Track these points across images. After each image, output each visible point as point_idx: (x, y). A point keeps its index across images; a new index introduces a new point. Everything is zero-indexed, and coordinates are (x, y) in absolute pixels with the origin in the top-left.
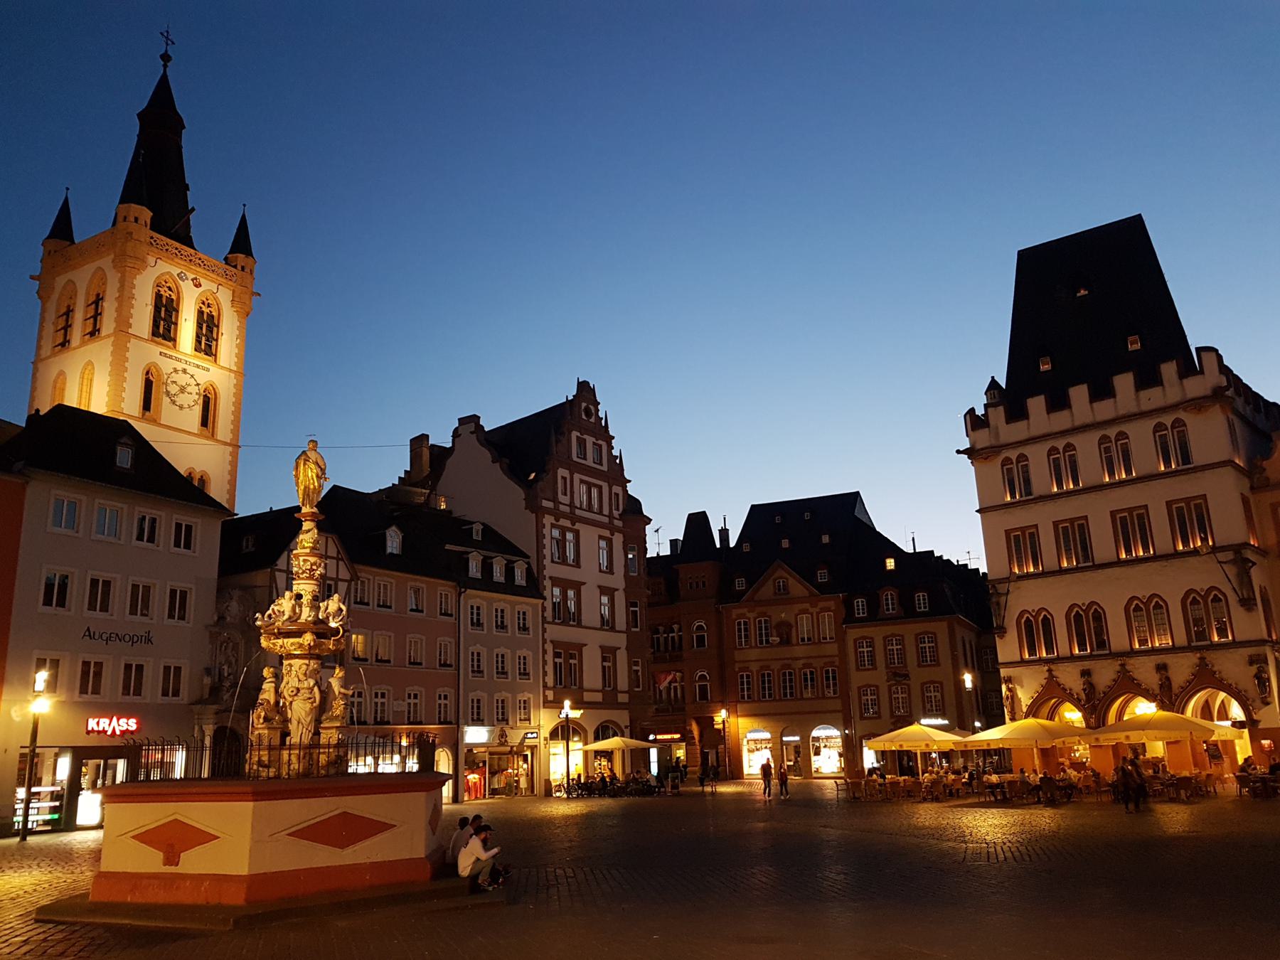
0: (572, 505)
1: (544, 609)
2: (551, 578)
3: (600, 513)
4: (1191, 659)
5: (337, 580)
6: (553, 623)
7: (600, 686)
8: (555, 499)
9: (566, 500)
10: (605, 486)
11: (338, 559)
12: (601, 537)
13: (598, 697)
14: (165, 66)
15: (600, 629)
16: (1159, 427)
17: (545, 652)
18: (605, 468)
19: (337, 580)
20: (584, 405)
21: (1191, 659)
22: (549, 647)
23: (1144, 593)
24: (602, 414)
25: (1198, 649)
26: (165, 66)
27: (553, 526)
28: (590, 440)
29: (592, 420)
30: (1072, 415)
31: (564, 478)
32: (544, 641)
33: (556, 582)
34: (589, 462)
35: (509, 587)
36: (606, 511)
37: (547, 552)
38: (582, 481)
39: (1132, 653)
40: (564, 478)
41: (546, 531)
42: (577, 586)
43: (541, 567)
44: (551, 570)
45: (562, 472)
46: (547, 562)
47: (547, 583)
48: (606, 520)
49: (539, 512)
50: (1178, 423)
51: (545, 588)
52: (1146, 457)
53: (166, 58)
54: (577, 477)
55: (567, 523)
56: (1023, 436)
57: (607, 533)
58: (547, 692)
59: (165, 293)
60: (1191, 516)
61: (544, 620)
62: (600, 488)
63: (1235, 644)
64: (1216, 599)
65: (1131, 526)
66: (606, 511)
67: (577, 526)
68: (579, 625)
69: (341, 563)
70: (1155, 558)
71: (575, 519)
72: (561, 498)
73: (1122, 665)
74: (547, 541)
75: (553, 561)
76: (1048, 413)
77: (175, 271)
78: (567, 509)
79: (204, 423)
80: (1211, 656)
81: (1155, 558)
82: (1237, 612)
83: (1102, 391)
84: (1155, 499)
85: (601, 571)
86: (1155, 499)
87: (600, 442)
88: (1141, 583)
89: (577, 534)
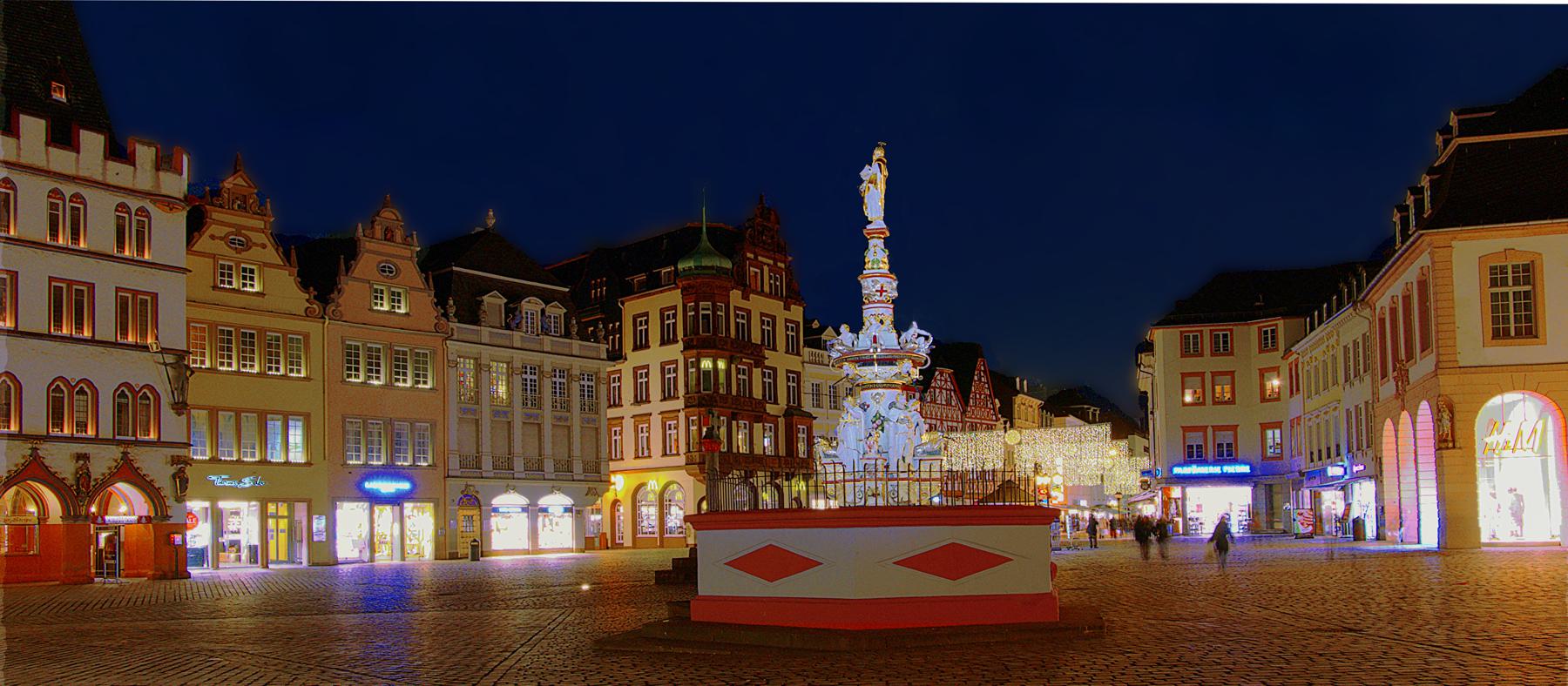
4: (115, 452)
16: (55, 193)
21: (115, 452)
23: (73, 376)
25: (120, 443)
30: (19, 148)
39: (47, 438)
50: (142, 211)
52: (100, 231)
56: (71, 171)
60: (137, 309)
63: (159, 443)
64: (82, 392)
65: (70, 301)
70: (92, 341)
73: (35, 449)
76: (48, 144)
80: (133, 452)
81: (92, 341)
82: (167, 412)
83: (118, 152)
84: (107, 280)
86: (107, 280)
88: (75, 363)
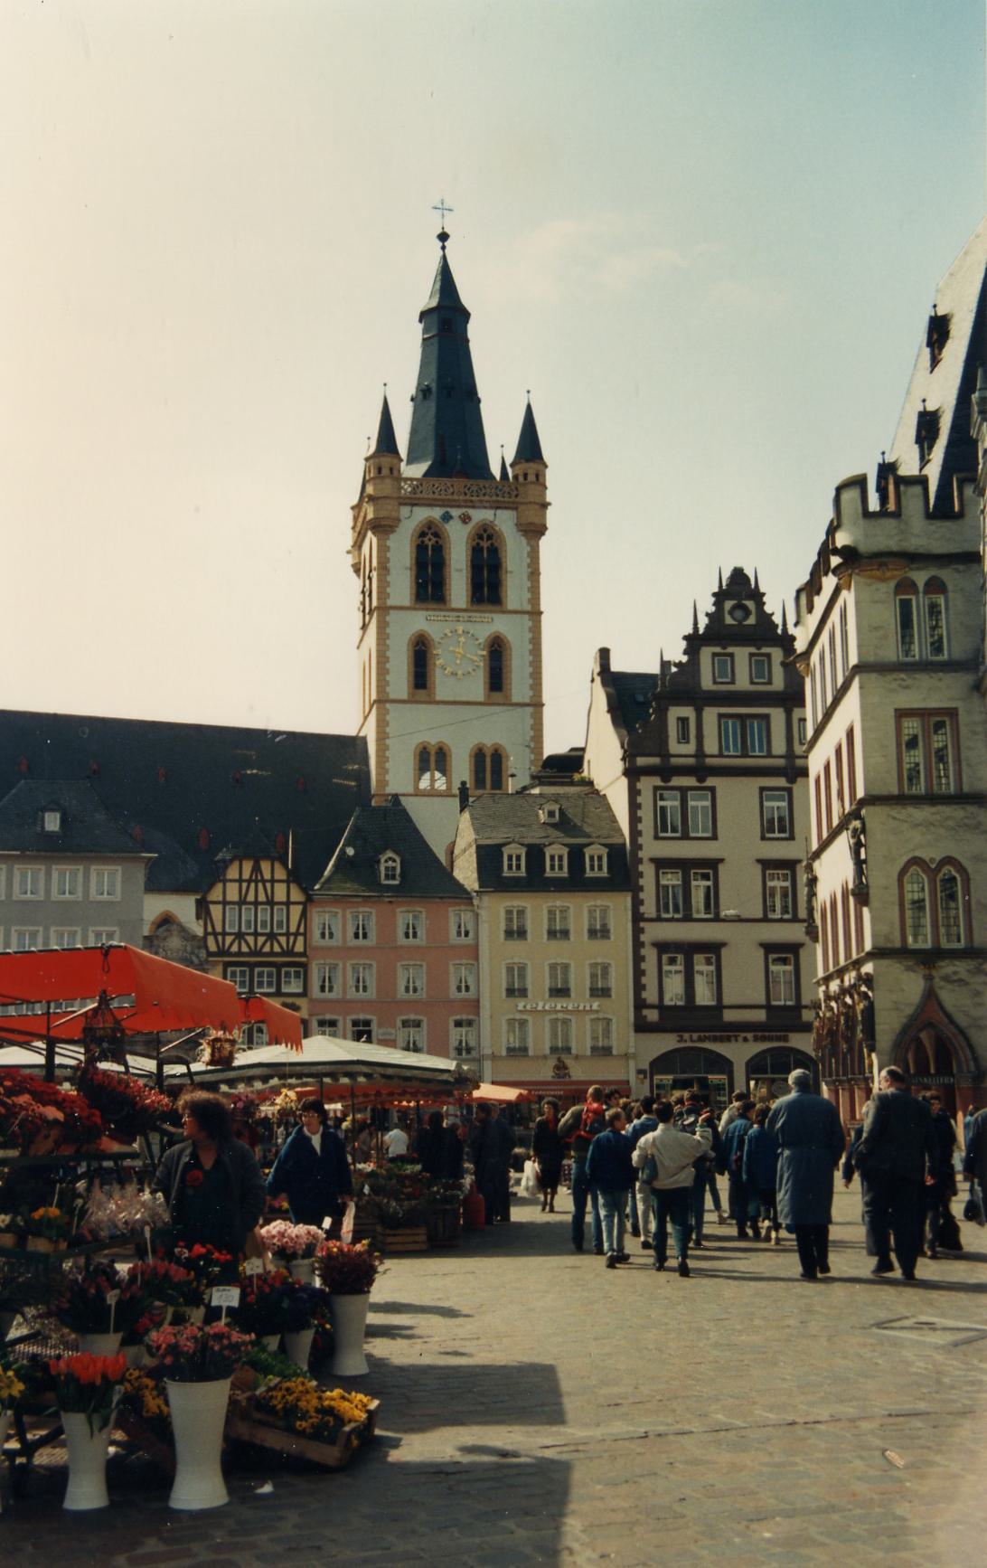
0: (700, 754)
1: (637, 903)
2: (652, 860)
3: (770, 755)
5: (288, 903)
6: (659, 919)
7: (762, 1000)
8: (665, 755)
9: (690, 748)
10: (777, 715)
11: (288, 882)
12: (762, 789)
13: (761, 1016)
14: (443, 248)
15: (765, 919)
17: (638, 959)
18: (778, 683)
19: (288, 903)
20: (728, 604)
22: (650, 954)
24: (768, 609)
26: (443, 248)
27: (656, 788)
28: (742, 654)
29: (751, 620)
31: (683, 721)
32: (638, 945)
33: (661, 864)
34: (743, 683)
35: (577, 882)
36: (779, 746)
37: (647, 826)
38: (721, 716)
40: (683, 721)
41: (646, 799)
42: (713, 864)
43: (636, 846)
44: (652, 848)
45: (675, 713)
46: (646, 839)
47: (647, 870)
48: (781, 762)
49: (632, 773)
51: (641, 875)
53: (443, 237)
54: (710, 714)
55: (690, 781)
57: (781, 782)
58: (645, 1012)
59: (430, 542)
61: (637, 918)
62: (767, 717)
66: (779, 746)
67: (710, 782)
68: (717, 919)
69: (292, 886)
71: (701, 770)
72: (674, 747)
74: (646, 814)
75: (656, 837)
77: (436, 513)
78: (691, 761)
79: (497, 679)
85: (763, 838)
87: (765, 650)
89: (712, 790)
